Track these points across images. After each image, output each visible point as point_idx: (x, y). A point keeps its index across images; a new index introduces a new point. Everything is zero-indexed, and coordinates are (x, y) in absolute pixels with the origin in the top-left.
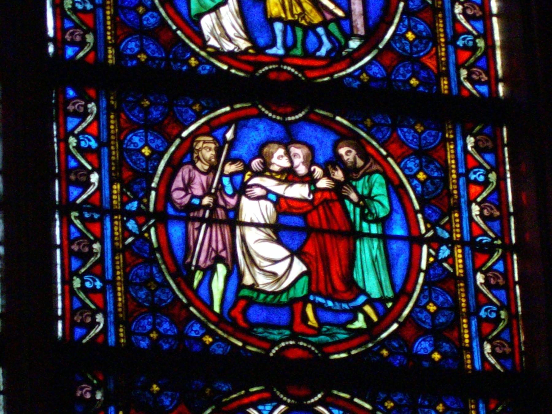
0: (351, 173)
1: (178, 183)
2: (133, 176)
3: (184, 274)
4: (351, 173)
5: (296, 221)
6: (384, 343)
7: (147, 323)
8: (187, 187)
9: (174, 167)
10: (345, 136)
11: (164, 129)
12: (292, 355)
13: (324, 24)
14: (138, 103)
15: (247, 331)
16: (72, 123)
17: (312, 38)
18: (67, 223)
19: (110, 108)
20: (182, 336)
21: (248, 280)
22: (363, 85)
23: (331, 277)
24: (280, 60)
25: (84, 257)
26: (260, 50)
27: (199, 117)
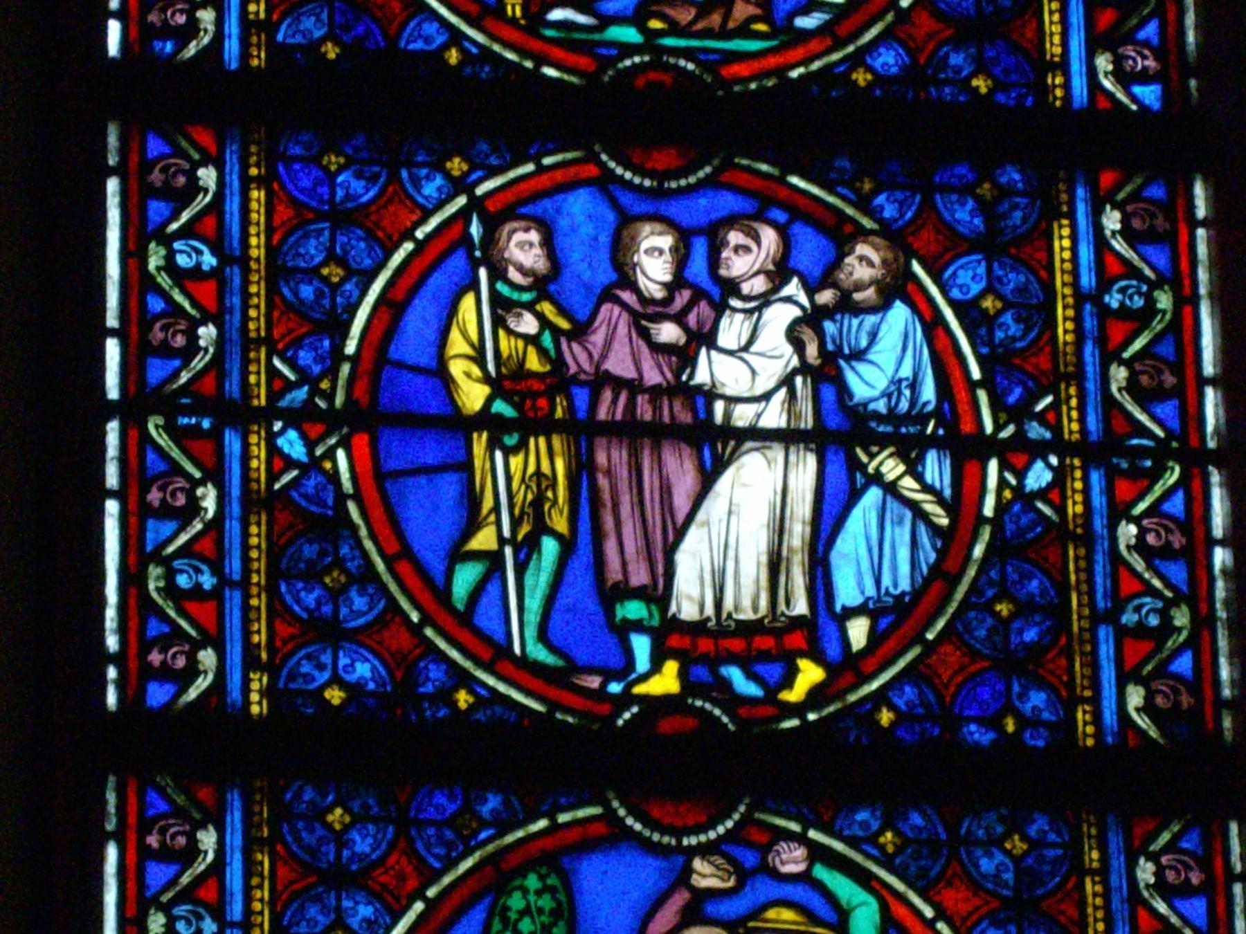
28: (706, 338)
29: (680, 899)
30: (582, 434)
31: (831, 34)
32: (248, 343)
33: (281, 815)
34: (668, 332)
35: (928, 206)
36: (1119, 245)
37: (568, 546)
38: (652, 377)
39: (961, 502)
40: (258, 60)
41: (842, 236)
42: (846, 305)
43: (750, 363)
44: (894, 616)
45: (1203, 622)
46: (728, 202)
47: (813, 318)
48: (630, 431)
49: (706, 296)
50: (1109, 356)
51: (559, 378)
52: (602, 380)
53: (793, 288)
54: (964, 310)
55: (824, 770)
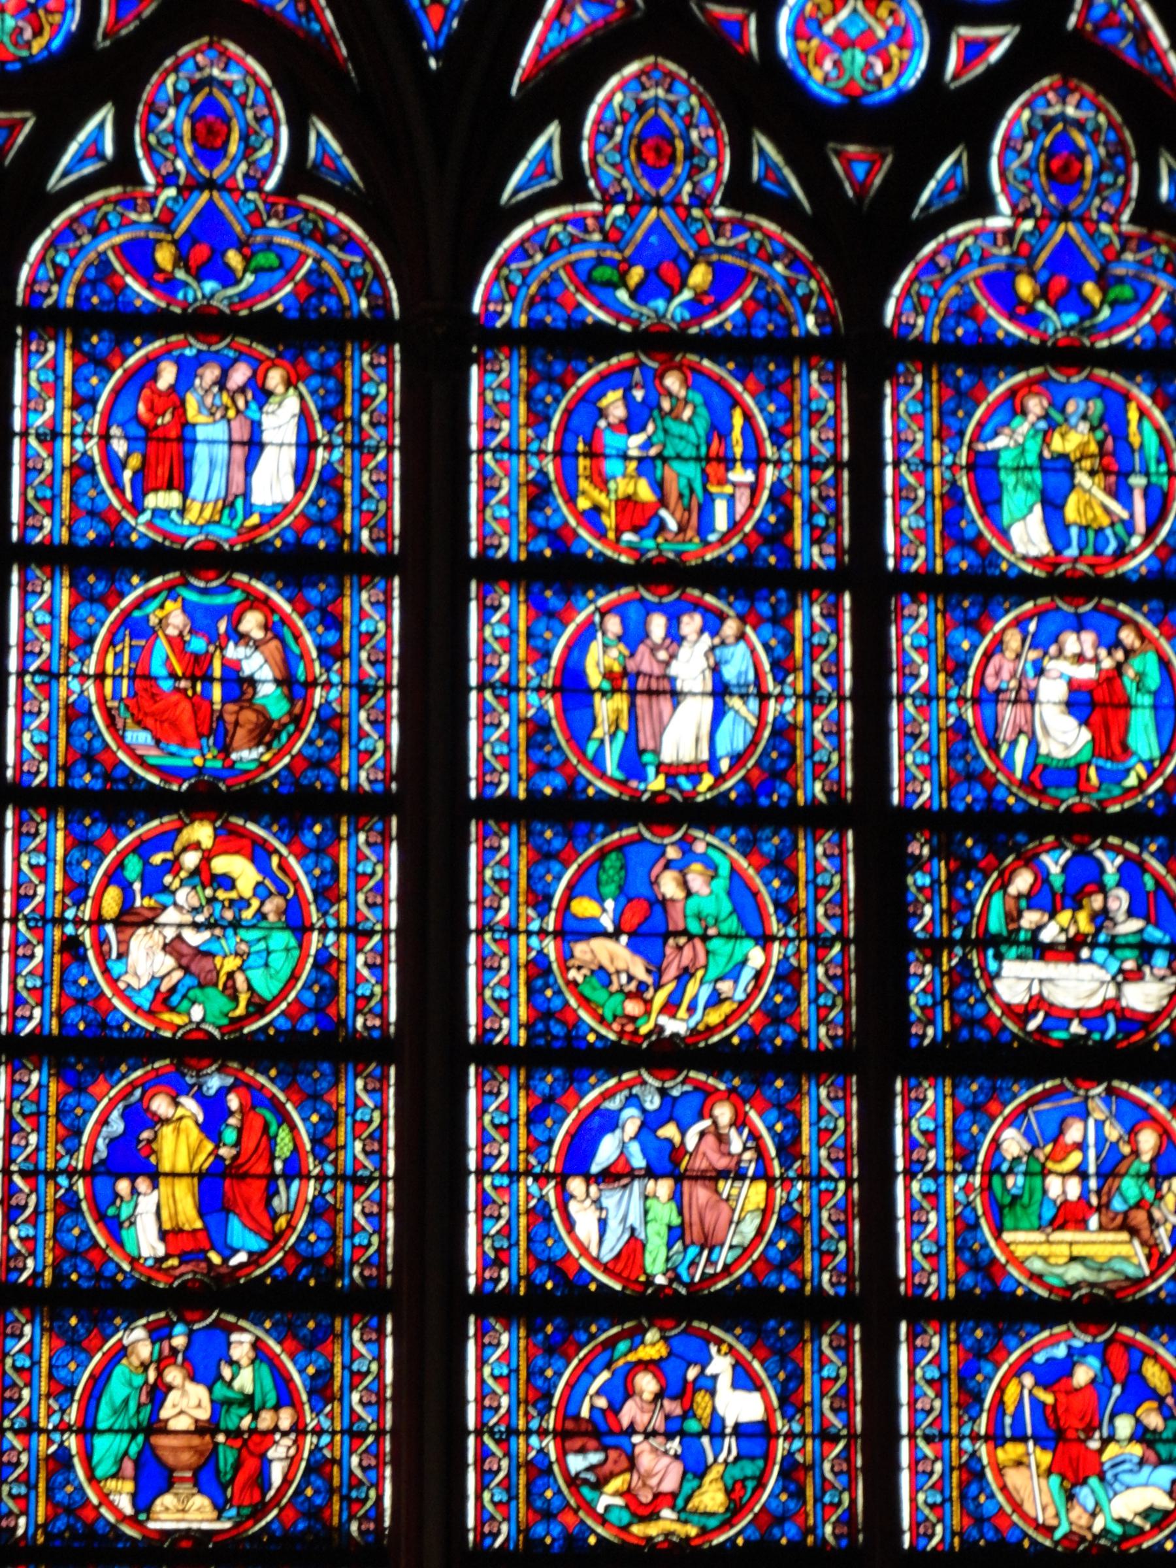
0: (1129, 653)
1: (990, 670)
2: (955, 668)
3: (993, 746)
4: (1129, 653)
5: (1084, 697)
6: (1149, 797)
7: (963, 789)
8: (997, 674)
9: (987, 656)
10: (1125, 621)
11: (978, 626)
12: (1077, 810)
13: (1112, 525)
14: (960, 603)
15: (1041, 793)
17: (1101, 539)
18: (902, 709)
19: (937, 611)
20: (990, 799)
21: (1043, 750)
22: (1142, 577)
23: (1110, 742)
24: (1075, 560)
25: (915, 736)
26: (1058, 551)
27: (1007, 611)
28: (673, 656)
29: (661, 863)
30: (633, 693)
33: (530, 834)
34: (662, 655)
35: (752, 607)
37: (627, 735)
38: (657, 670)
39: (761, 717)
40: (523, 556)
41: (722, 617)
42: (723, 643)
43: (690, 667)
44: (738, 760)
45: (842, 759)
47: (713, 649)
48: (650, 693)
49: (675, 637)
51: (625, 673)
53: (706, 636)
55: (712, 815)
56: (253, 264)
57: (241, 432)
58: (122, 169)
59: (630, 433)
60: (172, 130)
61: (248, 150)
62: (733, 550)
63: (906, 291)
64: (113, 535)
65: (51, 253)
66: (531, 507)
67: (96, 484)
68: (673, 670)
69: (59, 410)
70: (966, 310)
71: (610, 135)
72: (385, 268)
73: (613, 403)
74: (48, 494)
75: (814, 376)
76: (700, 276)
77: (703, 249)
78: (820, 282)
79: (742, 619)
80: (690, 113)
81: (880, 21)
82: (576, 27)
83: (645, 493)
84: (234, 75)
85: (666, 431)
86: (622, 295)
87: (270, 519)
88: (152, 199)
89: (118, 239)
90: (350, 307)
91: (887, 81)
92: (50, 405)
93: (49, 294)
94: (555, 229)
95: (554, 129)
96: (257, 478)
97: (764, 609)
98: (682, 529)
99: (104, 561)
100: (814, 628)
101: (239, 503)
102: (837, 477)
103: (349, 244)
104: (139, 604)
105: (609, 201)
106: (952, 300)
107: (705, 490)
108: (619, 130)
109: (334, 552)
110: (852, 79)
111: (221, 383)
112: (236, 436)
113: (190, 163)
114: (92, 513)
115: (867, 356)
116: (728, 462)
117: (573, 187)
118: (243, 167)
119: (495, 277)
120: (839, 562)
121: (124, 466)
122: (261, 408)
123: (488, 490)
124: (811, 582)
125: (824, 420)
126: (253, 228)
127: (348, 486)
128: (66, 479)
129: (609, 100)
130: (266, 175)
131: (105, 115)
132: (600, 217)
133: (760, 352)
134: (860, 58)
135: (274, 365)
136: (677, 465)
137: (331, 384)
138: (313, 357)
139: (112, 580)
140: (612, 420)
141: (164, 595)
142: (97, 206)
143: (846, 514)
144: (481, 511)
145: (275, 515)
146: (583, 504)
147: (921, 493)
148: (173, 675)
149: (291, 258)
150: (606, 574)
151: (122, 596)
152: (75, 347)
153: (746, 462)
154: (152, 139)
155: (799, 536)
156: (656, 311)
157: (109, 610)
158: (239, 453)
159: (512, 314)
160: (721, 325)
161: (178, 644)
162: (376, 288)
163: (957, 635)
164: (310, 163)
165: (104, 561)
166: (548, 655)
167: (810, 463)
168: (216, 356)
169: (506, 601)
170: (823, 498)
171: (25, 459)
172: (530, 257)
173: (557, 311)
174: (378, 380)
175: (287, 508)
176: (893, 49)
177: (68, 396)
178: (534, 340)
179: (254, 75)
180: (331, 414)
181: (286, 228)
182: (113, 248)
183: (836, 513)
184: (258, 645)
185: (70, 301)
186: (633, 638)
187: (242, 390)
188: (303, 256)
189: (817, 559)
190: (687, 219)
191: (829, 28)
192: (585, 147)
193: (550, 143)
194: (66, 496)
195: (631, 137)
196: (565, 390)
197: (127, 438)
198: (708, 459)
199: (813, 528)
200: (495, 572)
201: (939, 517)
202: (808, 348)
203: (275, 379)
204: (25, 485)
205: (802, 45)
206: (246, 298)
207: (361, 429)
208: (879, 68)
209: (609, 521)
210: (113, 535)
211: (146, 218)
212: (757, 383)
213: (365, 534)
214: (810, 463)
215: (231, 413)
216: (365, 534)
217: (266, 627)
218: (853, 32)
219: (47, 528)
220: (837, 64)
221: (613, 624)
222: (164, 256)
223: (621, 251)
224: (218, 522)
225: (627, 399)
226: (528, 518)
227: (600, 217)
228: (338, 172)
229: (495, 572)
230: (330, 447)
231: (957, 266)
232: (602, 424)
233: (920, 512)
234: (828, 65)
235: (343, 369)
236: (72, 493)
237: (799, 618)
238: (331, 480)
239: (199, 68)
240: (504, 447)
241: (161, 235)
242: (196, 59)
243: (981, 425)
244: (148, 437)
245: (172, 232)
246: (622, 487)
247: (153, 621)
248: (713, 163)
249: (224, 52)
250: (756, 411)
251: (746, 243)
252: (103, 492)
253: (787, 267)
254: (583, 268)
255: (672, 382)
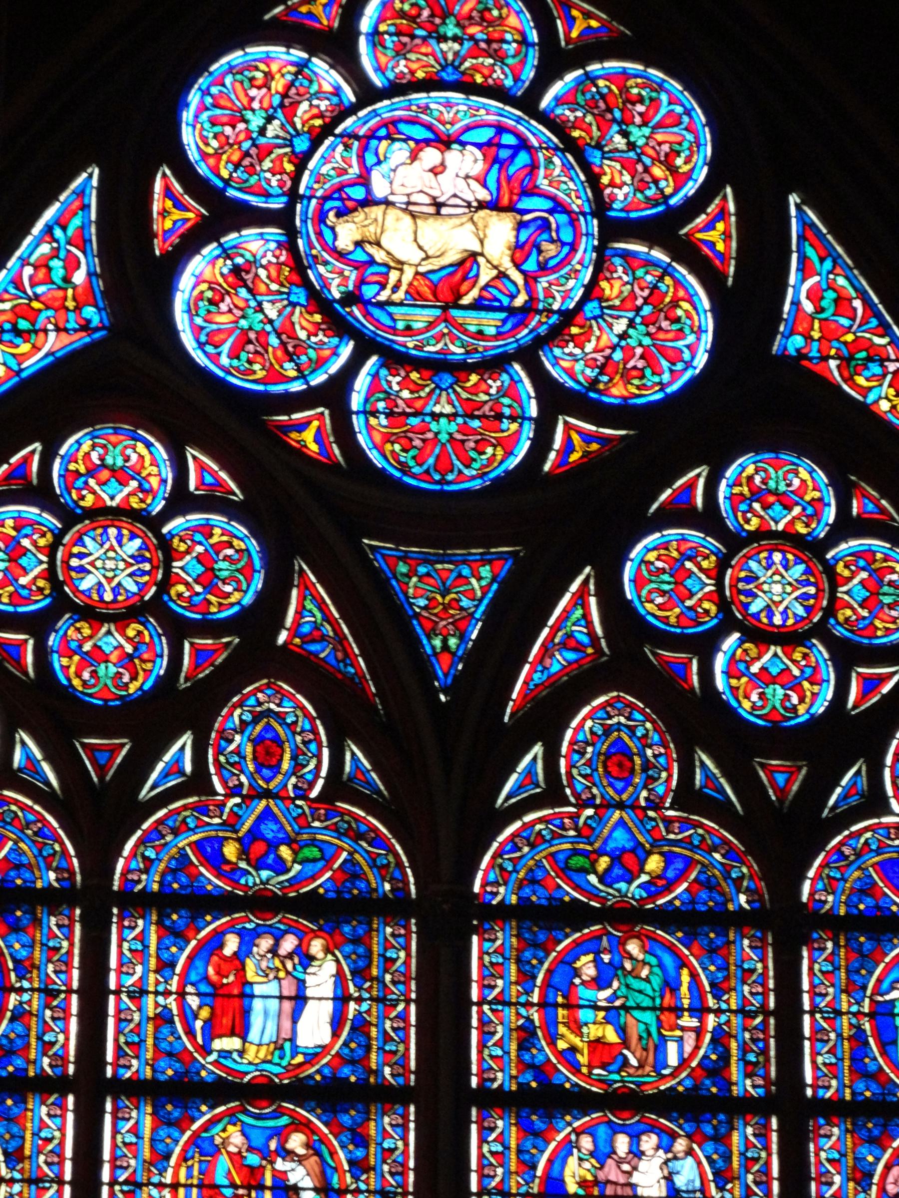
14: (865, 1125)
16: (823, 1141)
19: (847, 1131)
31: (673, 1075)
32: (511, 1173)
34: (626, 1167)
35: (698, 1127)
36: (752, 1138)
38: (622, 1180)
40: (514, 1088)
41: (674, 1136)
42: (675, 1158)
46: (642, 1127)
47: (666, 1162)
49: (637, 1154)
50: (748, 1171)
52: (608, 1182)
53: (661, 1152)
54: (708, 1158)
56: (301, 856)
57: (289, 989)
58: (198, 782)
59: (601, 988)
60: (237, 752)
61: (298, 767)
62: (683, 1082)
63: (818, 876)
64: (187, 1072)
65: (142, 848)
66: (521, 1048)
67: (173, 1032)
68: (636, 1178)
69: (146, 972)
70: (867, 889)
71: (582, 753)
72: (404, 859)
73: (586, 966)
74: (136, 1039)
75: (746, 942)
76: (654, 863)
77: (657, 843)
78: (750, 867)
79: (689, 1136)
80: (645, 736)
81: (795, 662)
82: (555, 668)
83: (611, 1036)
84: (287, 707)
85: (628, 986)
86: (593, 879)
87: (312, 1058)
88: (221, 806)
89: (194, 838)
90: (376, 890)
91: (801, 709)
92: (139, 969)
93: (139, 881)
94: (538, 827)
95: (538, 749)
96: (300, 1025)
97: (708, 1129)
98: (641, 1066)
99: (179, 1093)
100: (748, 1145)
101: (287, 1046)
102: (765, 1022)
103: (377, 840)
104: (206, 1127)
105: (582, 805)
106: (855, 881)
107: (660, 1033)
108: (590, 749)
109: (363, 1084)
110: (774, 708)
111: (274, 951)
112: (286, 993)
113: (251, 777)
114: (170, 1054)
115: (788, 927)
116: (677, 1011)
117: (553, 794)
118: (293, 780)
119: (491, 865)
120: (768, 1091)
121: (196, 1016)
122: (305, 968)
123: (486, 1033)
124: (746, 1107)
125: (754, 977)
126: (301, 828)
127: (374, 1032)
128: (150, 1028)
129: (581, 725)
130: (311, 785)
131: (186, 739)
132: (574, 817)
133: (702, 923)
134: (780, 692)
135: (317, 937)
136: (637, 1014)
137: (361, 950)
138: (347, 929)
139: (186, 1108)
140: (585, 978)
141: (226, 1120)
142: (177, 812)
143: (772, 1053)
144: (480, 1052)
145: (316, 1055)
146: (562, 1045)
147: (833, 1036)
148: (233, 1185)
149: (330, 851)
150: (581, 1102)
151: (193, 1120)
152: (159, 923)
153: (692, 1010)
154: (222, 759)
155: (735, 1071)
156: (619, 891)
157: (183, 1132)
158: (288, 1006)
159: (505, 894)
160: (670, 902)
161: (237, 1158)
162: (397, 874)
163: (863, 1150)
164: (345, 777)
165: (179, 1093)
166: (534, 1167)
167: (744, 1012)
168: (270, 931)
169: (500, 1123)
170: (754, 1040)
171: (118, 1011)
172: (520, 849)
173: (541, 891)
174: (399, 948)
175: (325, 1049)
176: (806, 685)
177: (153, 962)
178: (521, 914)
179: (303, 708)
180: (361, 974)
181: (326, 828)
182: (189, 845)
183: (765, 1052)
184: (301, 1160)
185: (156, 887)
186: (602, 1155)
187: (290, 956)
188: (341, 849)
189: (750, 1089)
190: (643, 819)
191: (755, 668)
192: (563, 762)
193: (535, 759)
194: (150, 1041)
195: (599, 754)
196: (548, 954)
197: (199, 994)
198: (662, 1009)
199: (747, 1063)
200: (492, 1100)
201: (847, 1055)
202: (741, 920)
203: (316, 947)
204: (118, 1032)
205: (734, 682)
206: (295, 882)
207: (385, 986)
208: (795, 699)
209: (583, 1059)
210: (187, 1072)
211: (217, 821)
212: (702, 948)
213: (387, 1071)
214: (744, 1012)
215: (282, 974)
216: (387, 1071)
217: (308, 1145)
218: (774, 671)
219: (136, 1068)
220: (762, 696)
221: (586, 1142)
222: (230, 851)
223: (591, 844)
224: (270, 1062)
225: (597, 962)
226: (518, 1056)
227: (574, 817)
228: (369, 783)
229: (492, 1100)
230: (359, 1000)
231: (859, 855)
232: (577, 981)
233: (832, 1051)
234: (754, 697)
235: (371, 938)
236: (155, 1038)
237: (736, 1138)
238: (361, 1026)
239: (260, 704)
240: (501, 1000)
241: (229, 834)
242: (257, 695)
243: (879, 981)
244: (216, 994)
245: (236, 832)
246: (594, 1032)
247: (218, 1140)
248: (664, 775)
249: (279, 691)
250: (700, 971)
251: (690, 836)
252: (179, 1038)
253: (723, 856)
254: (561, 857)
255: (633, 947)
